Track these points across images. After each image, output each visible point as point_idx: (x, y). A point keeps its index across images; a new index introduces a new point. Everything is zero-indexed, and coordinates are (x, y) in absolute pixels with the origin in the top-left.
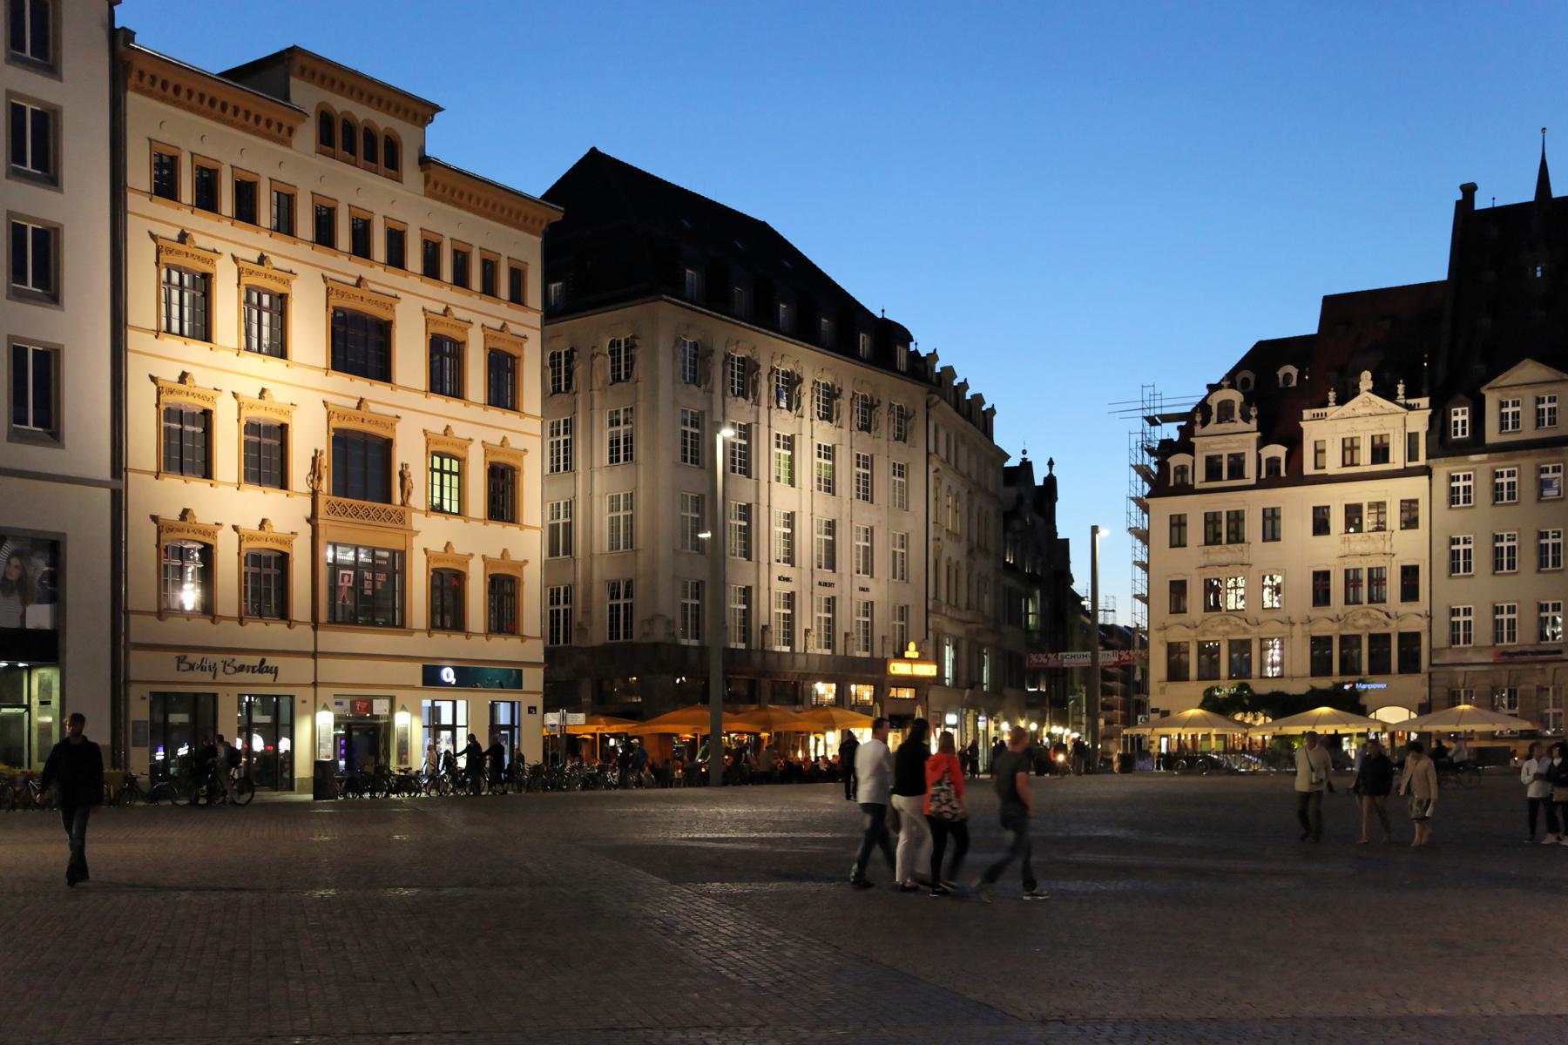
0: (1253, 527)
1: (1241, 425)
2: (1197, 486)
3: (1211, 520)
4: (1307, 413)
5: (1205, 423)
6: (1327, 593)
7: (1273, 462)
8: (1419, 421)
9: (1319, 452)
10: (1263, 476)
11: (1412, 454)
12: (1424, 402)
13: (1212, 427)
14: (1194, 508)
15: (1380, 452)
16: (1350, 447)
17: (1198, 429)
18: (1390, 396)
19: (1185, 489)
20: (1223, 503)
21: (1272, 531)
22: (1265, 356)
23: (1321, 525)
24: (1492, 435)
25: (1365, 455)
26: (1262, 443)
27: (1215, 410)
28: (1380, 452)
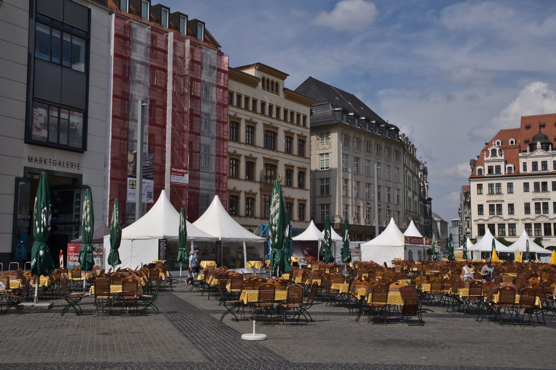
1: (499, 157)
2: (486, 175)
4: (520, 155)
5: (487, 156)
7: (510, 168)
16: (535, 165)
17: (485, 159)
19: (481, 177)
22: (503, 134)
26: (506, 162)
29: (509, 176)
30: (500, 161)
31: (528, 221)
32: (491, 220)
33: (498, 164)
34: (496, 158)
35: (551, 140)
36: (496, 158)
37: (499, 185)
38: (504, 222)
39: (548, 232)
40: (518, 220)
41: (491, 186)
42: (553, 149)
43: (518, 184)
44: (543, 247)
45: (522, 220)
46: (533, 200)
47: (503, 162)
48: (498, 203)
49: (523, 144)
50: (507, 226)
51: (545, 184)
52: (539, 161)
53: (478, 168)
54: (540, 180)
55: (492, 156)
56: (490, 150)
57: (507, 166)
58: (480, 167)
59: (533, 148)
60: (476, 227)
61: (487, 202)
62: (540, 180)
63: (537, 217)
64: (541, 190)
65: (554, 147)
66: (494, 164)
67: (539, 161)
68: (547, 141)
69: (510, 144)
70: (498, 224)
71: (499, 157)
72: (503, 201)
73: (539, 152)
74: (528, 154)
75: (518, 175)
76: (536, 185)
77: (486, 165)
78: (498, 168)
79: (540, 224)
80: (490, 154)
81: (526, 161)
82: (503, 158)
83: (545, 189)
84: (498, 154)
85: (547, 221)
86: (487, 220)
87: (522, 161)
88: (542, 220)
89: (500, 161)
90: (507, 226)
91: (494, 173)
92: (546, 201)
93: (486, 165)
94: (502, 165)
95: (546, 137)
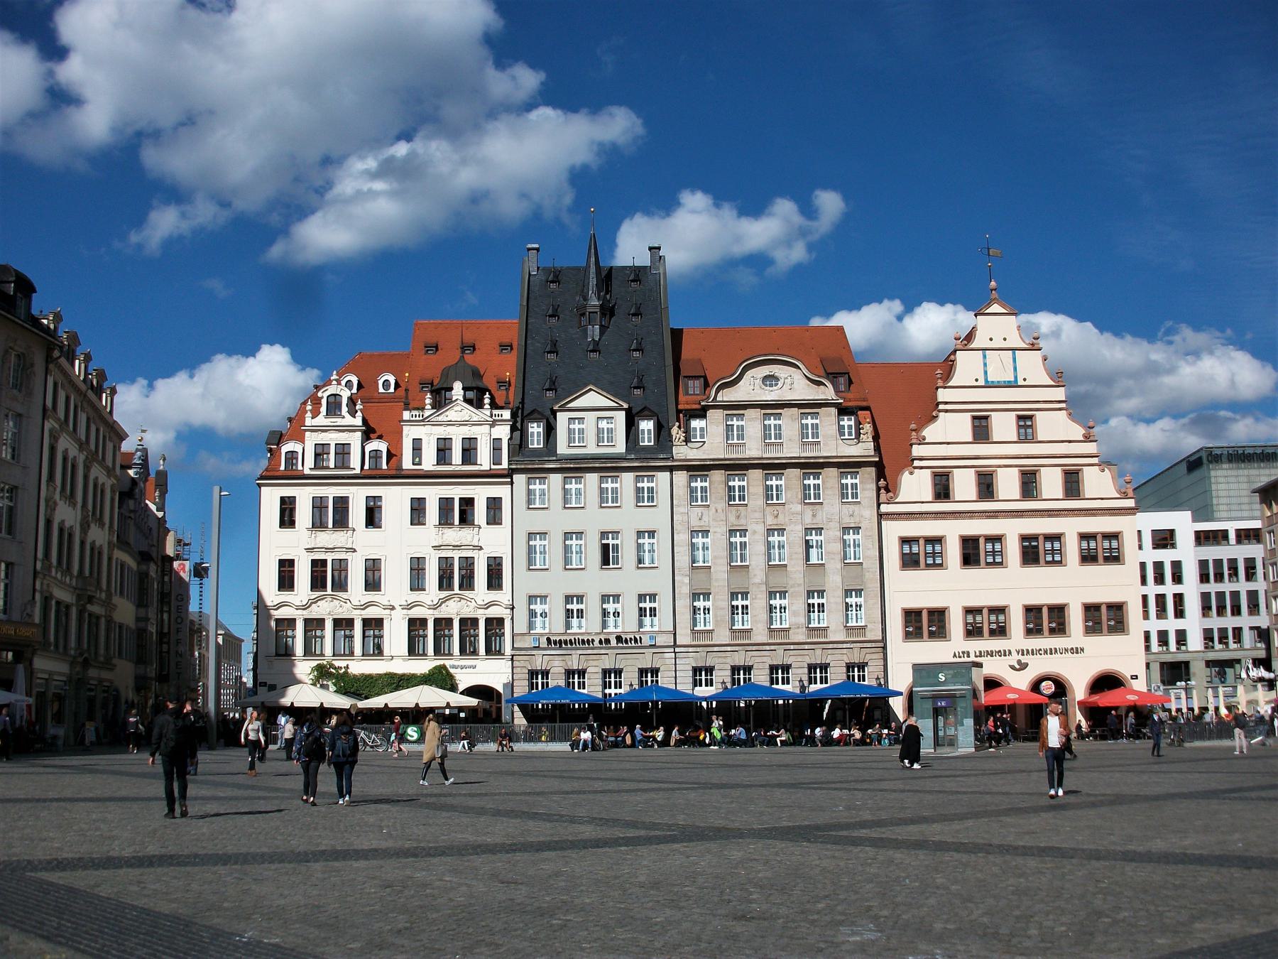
0: (357, 514)
1: (349, 420)
2: (307, 471)
3: (319, 505)
4: (406, 415)
5: (315, 414)
7: (376, 455)
8: (503, 432)
10: (366, 467)
11: (497, 460)
12: (507, 414)
13: (321, 420)
14: (304, 497)
17: (309, 421)
18: (479, 405)
20: (331, 492)
21: (372, 518)
24: (562, 448)
25: (457, 455)
27: (324, 402)
29: (371, 475)
30: (350, 429)
31: (417, 613)
33: (342, 438)
34: (339, 421)
35: (489, 381)
36: (339, 421)
42: (494, 405)
43: (396, 499)
44: (453, 688)
46: (437, 548)
47: (359, 434)
49: (415, 388)
51: (468, 503)
52: (457, 436)
53: (286, 448)
54: (457, 492)
55: (329, 414)
56: (324, 395)
57: (370, 446)
59: (441, 402)
61: (309, 550)
62: (457, 492)
65: (500, 402)
66: (332, 438)
67: (457, 436)
68: (480, 385)
69: (381, 390)
71: (349, 420)
73: (459, 410)
74: (427, 413)
75: (397, 475)
76: (446, 504)
77: (311, 440)
78: (343, 450)
79: (449, 622)
80: (323, 409)
81: (422, 434)
82: (358, 421)
83: (466, 519)
84: (345, 409)
85: (468, 612)
87: (410, 433)
88: (455, 609)
89: (350, 429)
90: (358, 626)
91: (332, 465)
94: (355, 440)
95: (477, 374)
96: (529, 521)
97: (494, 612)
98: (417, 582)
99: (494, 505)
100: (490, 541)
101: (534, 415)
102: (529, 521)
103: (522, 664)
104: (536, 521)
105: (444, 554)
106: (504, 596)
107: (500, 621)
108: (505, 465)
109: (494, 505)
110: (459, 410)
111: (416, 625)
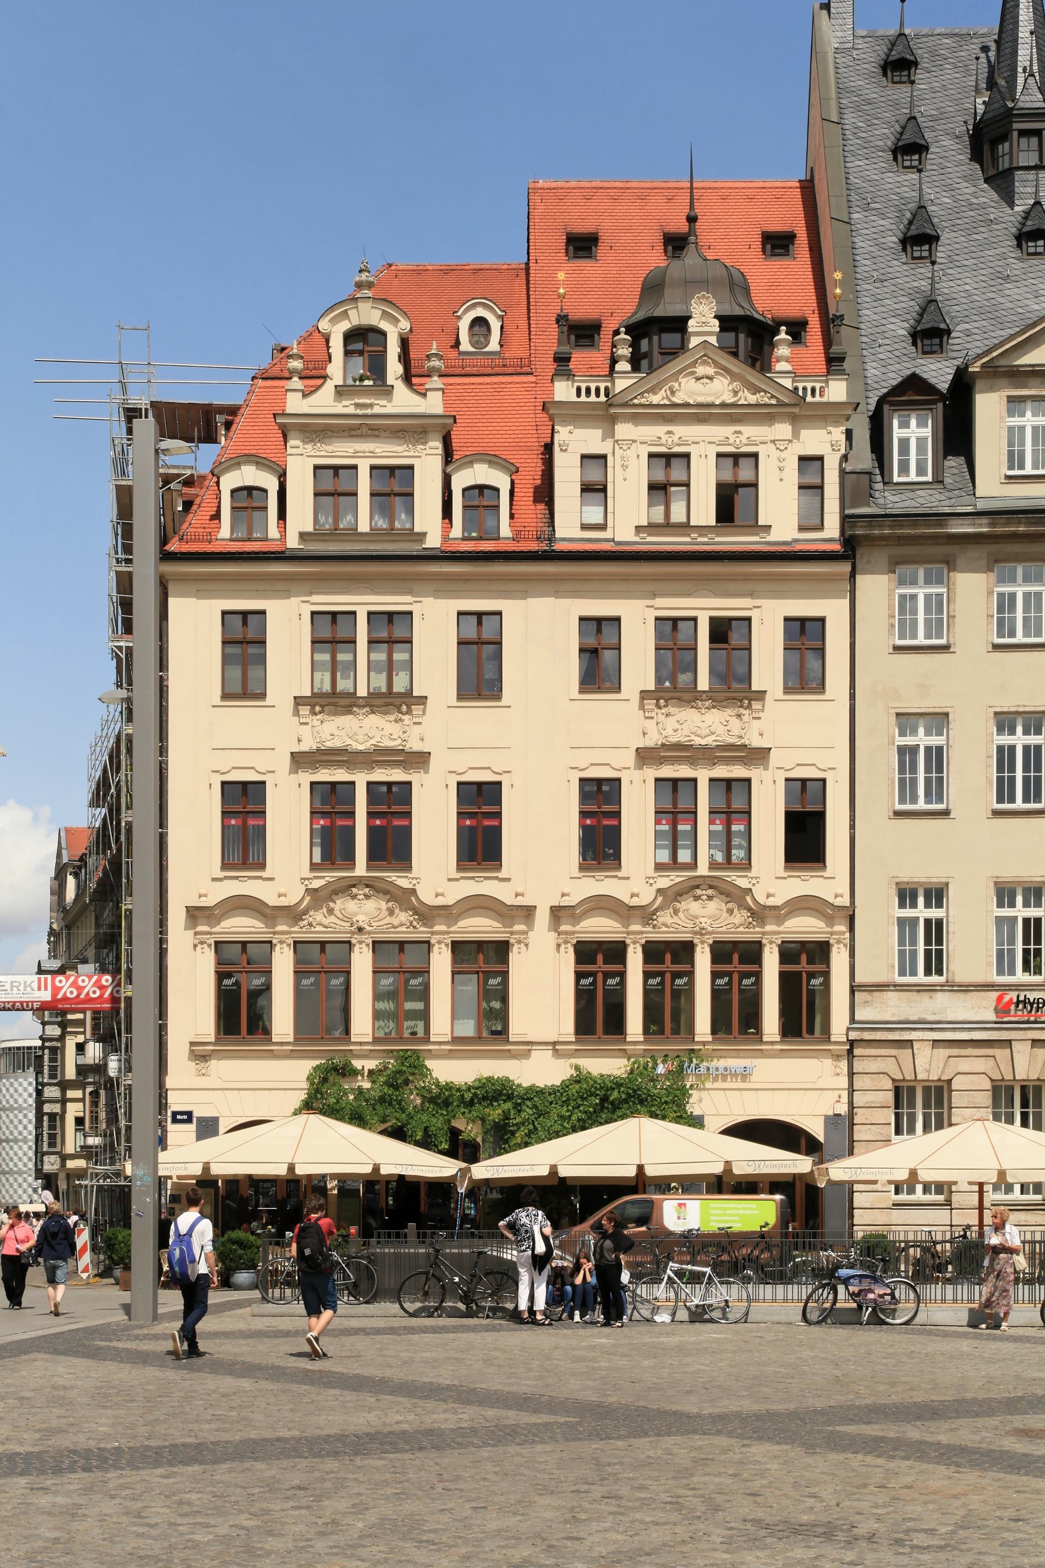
6: (615, 834)
9: (594, 490)
15: (733, 502)
23: (598, 667)
28: (733, 502)
31: (601, 927)
32: (318, 916)
37: (393, 631)
38: (421, 933)
39: (737, 1018)
40: (528, 912)
41: (331, 633)
45: (558, 913)
46: (646, 756)
48: (380, 775)
50: (441, 963)
58: (250, 475)
60: (206, 963)
63: (672, 896)
64: (703, 683)
70: (377, 945)
72: (420, 760)
79: (684, 951)
86: (293, 914)
87: (574, 442)
88: (706, 919)
90: (441, 963)
92: (738, 771)
93: (301, 462)
94: (427, 464)
96: (898, 682)
97: (806, 927)
98: (600, 844)
99: (805, 636)
100: (795, 735)
101: (911, 392)
102: (898, 682)
103: (874, 1066)
104: (918, 682)
105: (668, 771)
106: (828, 883)
107: (820, 951)
108: (832, 528)
109: (805, 636)
110: (705, 380)
111: (598, 960)
